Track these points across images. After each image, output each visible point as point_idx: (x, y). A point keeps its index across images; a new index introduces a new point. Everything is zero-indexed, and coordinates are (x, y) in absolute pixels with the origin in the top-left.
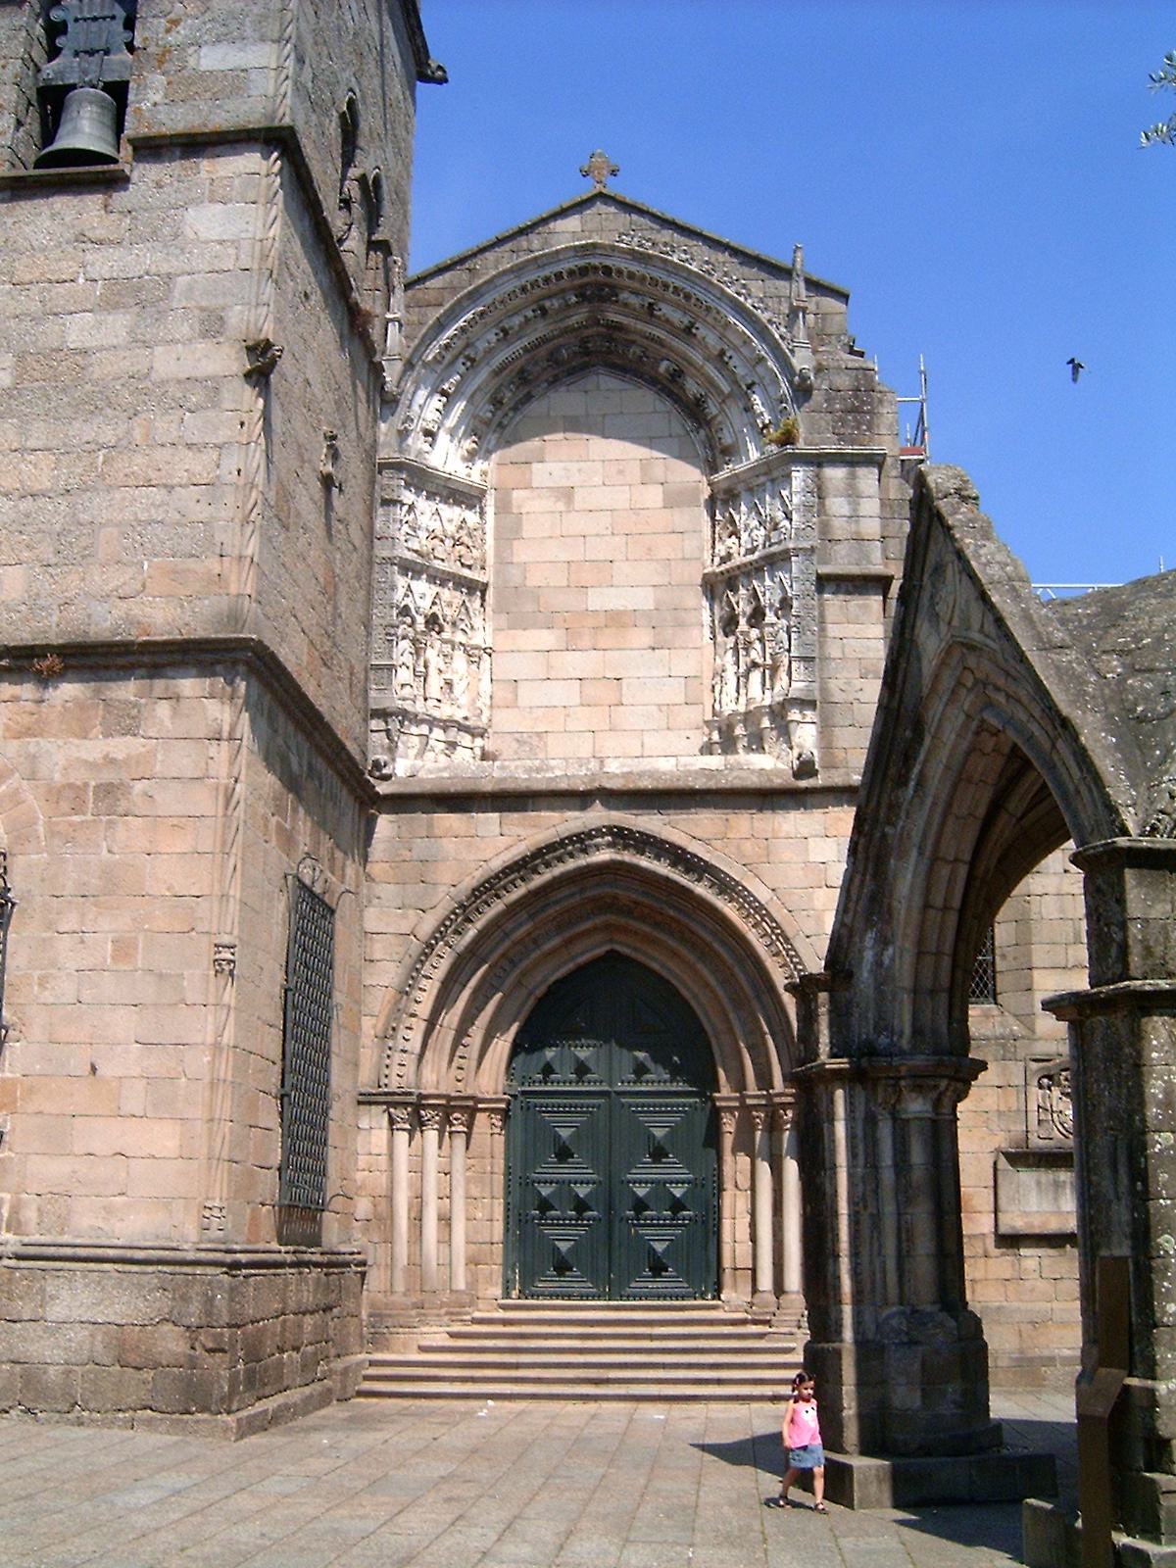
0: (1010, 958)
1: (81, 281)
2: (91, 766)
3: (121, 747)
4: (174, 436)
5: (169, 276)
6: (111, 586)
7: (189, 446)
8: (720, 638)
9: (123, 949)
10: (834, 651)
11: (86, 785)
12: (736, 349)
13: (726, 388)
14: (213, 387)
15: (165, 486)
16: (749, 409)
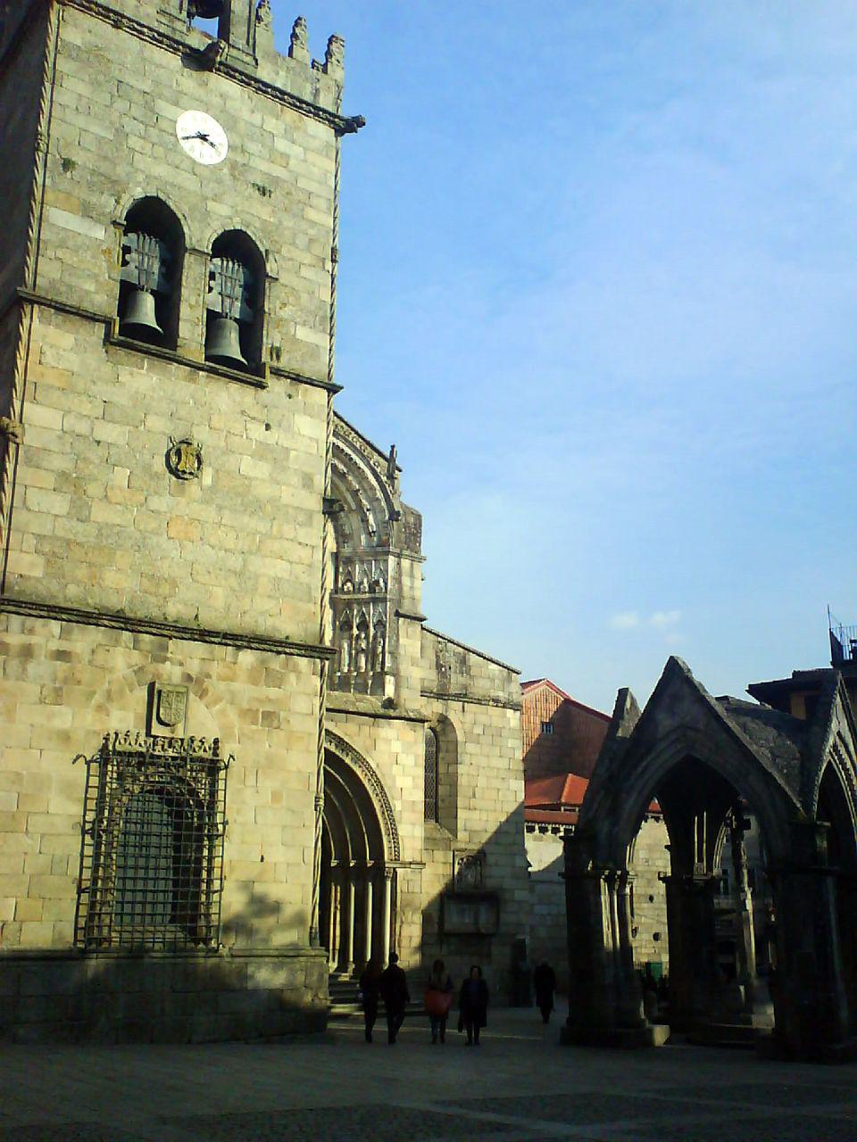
0: (447, 803)
1: (245, 437)
2: (260, 701)
3: (273, 692)
4: (291, 536)
5: (287, 448)
6: (267, 607)
7: (300, 544)
8: (338, 631)
9: (276, 796)
10: (402, 652)
11: (258, 710)
12: (365, 491)
13: (354, 507)
14: (310, 514)
15: (289, 562)
16: (365, 520)
